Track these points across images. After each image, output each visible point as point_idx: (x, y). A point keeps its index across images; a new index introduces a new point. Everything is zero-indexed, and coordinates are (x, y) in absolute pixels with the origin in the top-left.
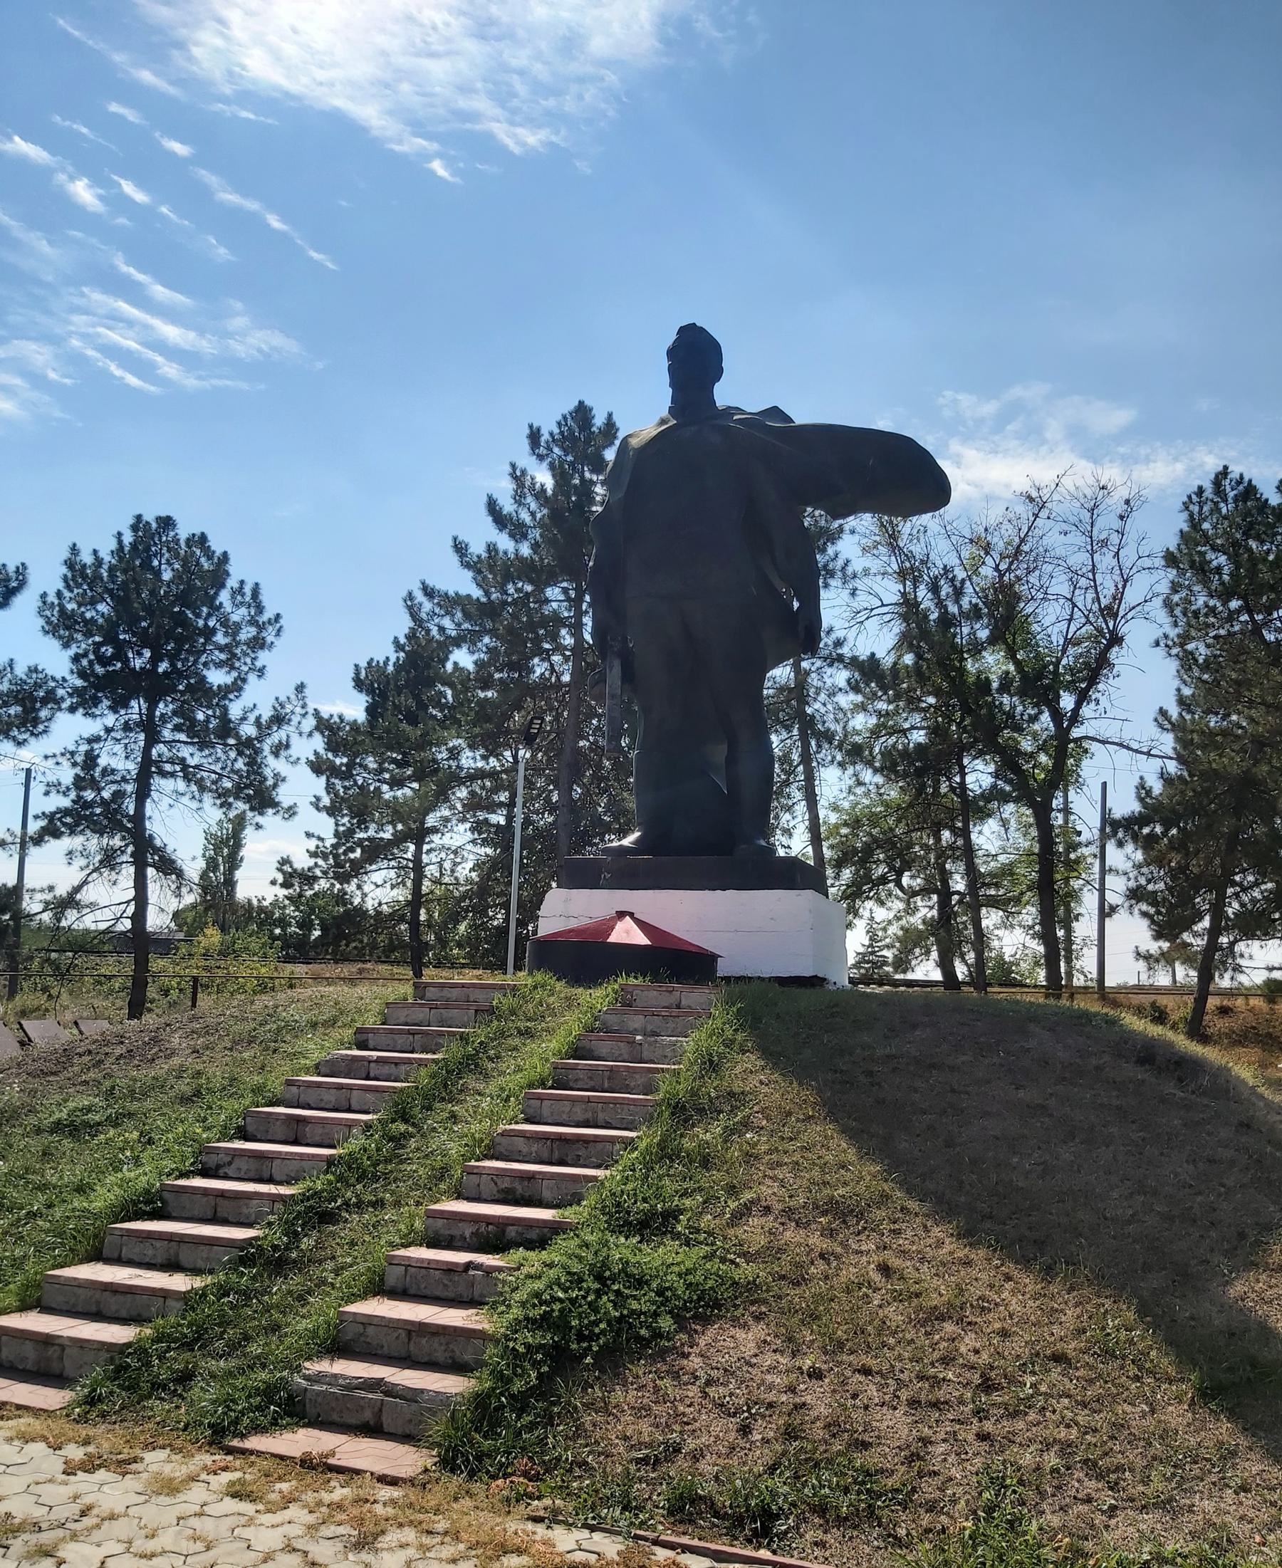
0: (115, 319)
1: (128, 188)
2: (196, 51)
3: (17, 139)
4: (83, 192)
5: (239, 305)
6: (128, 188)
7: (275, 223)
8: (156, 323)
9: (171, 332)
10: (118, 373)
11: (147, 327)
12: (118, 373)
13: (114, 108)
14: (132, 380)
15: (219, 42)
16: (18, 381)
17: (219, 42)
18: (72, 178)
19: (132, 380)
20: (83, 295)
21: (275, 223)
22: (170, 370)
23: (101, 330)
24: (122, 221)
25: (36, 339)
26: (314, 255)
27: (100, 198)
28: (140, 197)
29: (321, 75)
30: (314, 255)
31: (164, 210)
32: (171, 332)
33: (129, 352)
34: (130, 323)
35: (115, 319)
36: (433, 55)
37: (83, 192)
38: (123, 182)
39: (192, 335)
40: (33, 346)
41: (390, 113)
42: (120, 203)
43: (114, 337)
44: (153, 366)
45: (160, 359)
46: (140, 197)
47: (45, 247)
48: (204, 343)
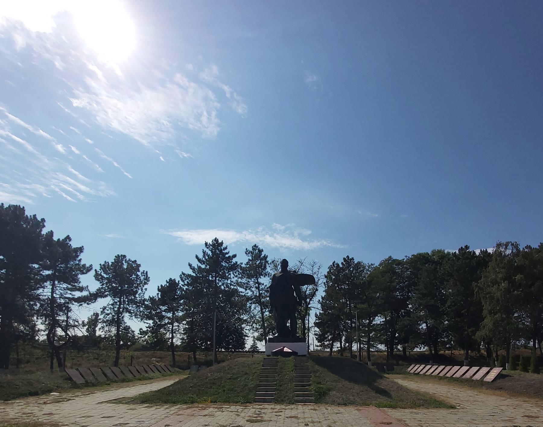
0: (65, 182)
1: (73, 149)
2: (98, 118)
3: (41, 131)
4: (60, 148)
5: (103, 183)
6: (73, 149)
7: (116, 165)
8: (78, 184)
9: (82, 188)
10: (65, 196)
11: (75, 185)
12: (65, 196)
13: (71, 128)
14: (69, 198)
15: (104, 117)
16: (33, 195)
17: (104, 117)
18: (57, 144)
19: (69, 198)
20: (56, 174)
21: (116, 165)
22: (81, 197)
23: (61, 184)
24: (71, 157)
25: (40, 184)
26: (125, 173)
27: (65, 150)
28: (77, 152)
29: (132, 130)
30: (125, 173)
31: (84, 156)
32: (82, 188)
33: (69, 191)
34: (70, 184)
35: (65, 182)
36: (162, 131)
37: (60, 148)
38: (72, 147)
39: (88, 189)
40: (39, 186)
41: (149, 143)
42: (71, 152)
43: (65, 187)
44: (76, 195)
45: (78, 194)
46: (77, 152)
47: (46, 161)
48: (92, 191)
